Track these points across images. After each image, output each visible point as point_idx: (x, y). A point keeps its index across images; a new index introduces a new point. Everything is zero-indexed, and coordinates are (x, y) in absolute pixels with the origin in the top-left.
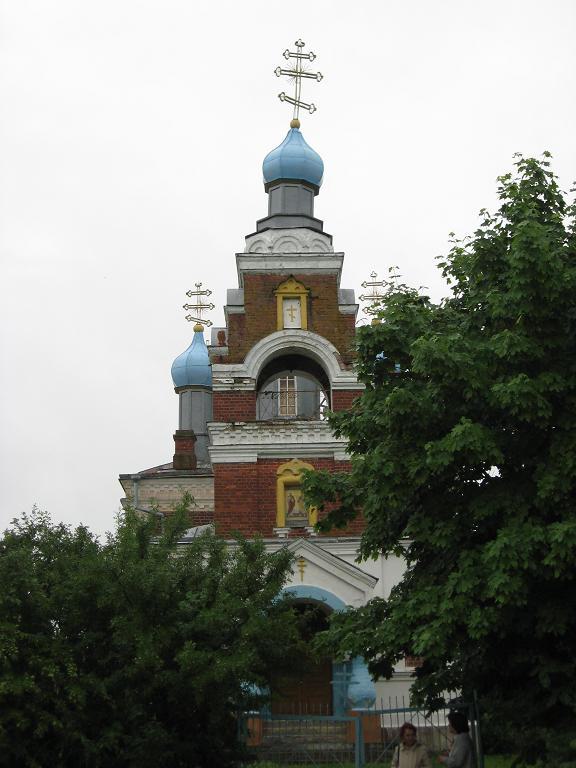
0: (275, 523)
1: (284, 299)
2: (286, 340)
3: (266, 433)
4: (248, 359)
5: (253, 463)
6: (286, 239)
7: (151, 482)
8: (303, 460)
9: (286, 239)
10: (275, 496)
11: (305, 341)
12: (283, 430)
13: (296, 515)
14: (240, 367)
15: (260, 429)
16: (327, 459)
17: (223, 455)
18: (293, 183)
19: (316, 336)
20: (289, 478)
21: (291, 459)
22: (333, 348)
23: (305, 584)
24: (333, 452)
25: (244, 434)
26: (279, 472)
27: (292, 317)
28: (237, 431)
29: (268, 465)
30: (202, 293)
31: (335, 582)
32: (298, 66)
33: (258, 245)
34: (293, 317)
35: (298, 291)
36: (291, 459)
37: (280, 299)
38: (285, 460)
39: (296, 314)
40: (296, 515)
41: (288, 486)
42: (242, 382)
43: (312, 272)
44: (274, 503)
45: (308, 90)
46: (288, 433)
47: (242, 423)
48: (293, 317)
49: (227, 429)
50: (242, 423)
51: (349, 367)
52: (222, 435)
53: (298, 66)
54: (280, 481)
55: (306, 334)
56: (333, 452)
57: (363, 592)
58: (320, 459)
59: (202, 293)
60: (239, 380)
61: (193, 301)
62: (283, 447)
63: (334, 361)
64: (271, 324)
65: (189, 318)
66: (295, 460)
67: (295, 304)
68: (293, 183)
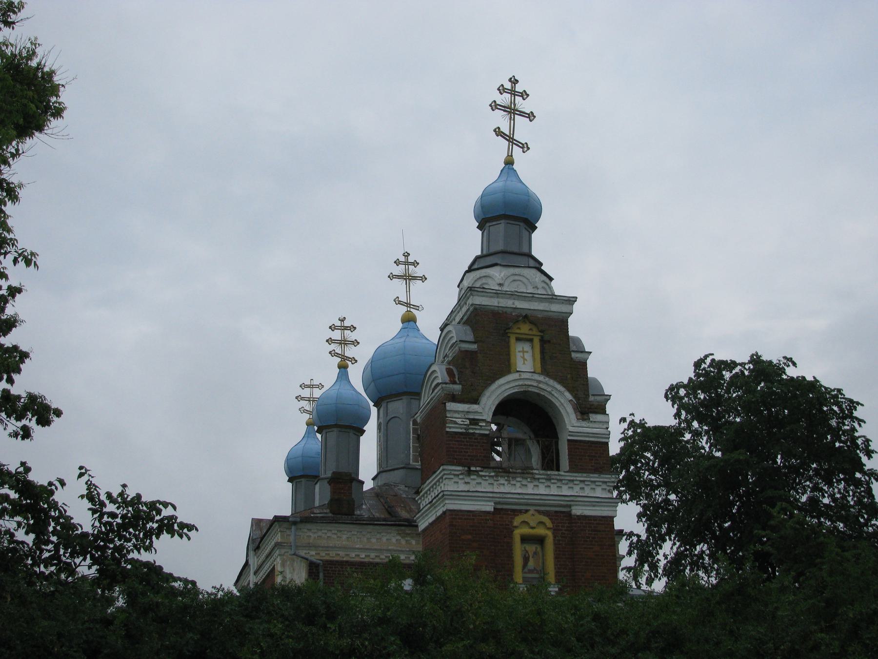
0: (512, 579)
1: (518, 339)
2: (521, 383)
3: (502, 481)
4: (483, 400)
5: (488, 512)
6: (516, 278)
7: (309, 526)
8: (539, 512)
9: (516, 278)
10: (511, 550)
11: (541, 385)
12: (519, 479)
13: (531, 571)
14: (475, 407)
15: (496, 476)
16: (561, 512)
17: (453, 502)
18: (509, 219)
19: (552, 382)
20: (526, 530)
21: (527, 511)
22: (569, 396)
24: (570, 506)
25: (479, 480)
27: (525, 360)
28: (472, 477)
29: (504, 515)
30: (346, 328)
32: (512, 101)
33: (484, 280)
34: (525, 360)
35: (530, 332)
36: (527, 511)
37: (513, 340)
38: (520, 512)
39: (528, 356)
40: (531, 571)
41: (525, 539)
42: (477, 424)
44: (510, 557)
45: (523, 129)
46: (524, 482)
47: (478, 469)
48: (525, 360)
49: (462, 474)
51: (586, 417)
52: (456, 479)
53: (512, 101)
54: (517, 533)
55: (541, 378)
56: (570, 506)
58: (556, 512)
59: (346, 328)
60: (474, 422)
61: (337, 335)
62: (521, 496)
63: (570, 409)
64: (505, 367)
65: (332, 353)
66: (531, 512)
67: (527, 347)
68: (509, 219)
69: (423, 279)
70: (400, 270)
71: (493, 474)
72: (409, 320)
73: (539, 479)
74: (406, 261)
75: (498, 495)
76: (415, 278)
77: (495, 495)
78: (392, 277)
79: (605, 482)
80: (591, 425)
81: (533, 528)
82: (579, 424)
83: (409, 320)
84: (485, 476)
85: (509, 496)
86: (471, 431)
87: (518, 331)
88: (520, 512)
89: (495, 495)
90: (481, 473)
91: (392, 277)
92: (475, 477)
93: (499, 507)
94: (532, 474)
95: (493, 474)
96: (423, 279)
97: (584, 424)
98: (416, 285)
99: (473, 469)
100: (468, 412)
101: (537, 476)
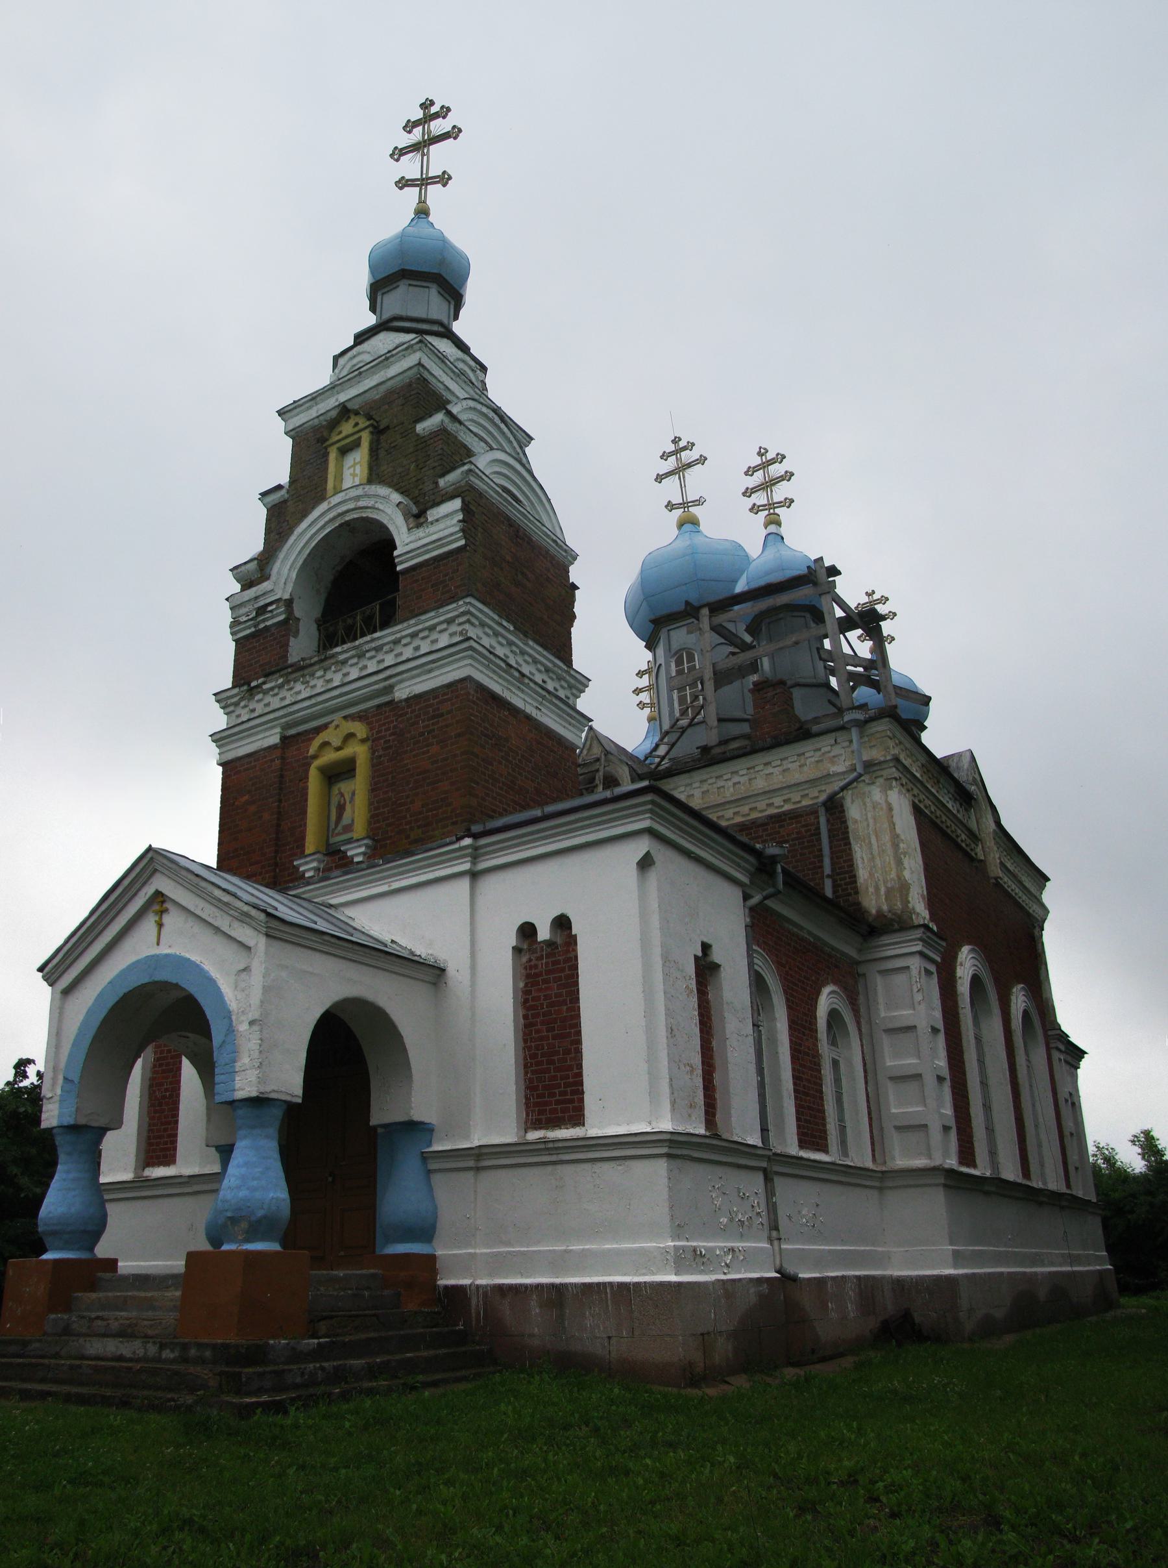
3: (299, 687)
9: (355, 361)
11: (361, 504)
15: (288, 682)
18: (418, 283)
20: (329, 757)
22: (396, 497)
23: (164, 950)
26: (312, 751)
31: (207, 936)
43: (383, 389)
45: (440, 157)
47: (260, 681)
49: (242, 699)
50: (260, 681)
51: (422, 520)
57: (249, 948)
58: (379, 706)
62: (313, 701)
68: (418, 283)
69: (702, 460)
70: (671, 463)
71: (281, 681)
72: (689, 523)
73: (344, 662)
74: (679, 447)
75: (281, 713)
76: (689, 465)
77: (277, 714)
78: (660, 478)
79: (449, 622)
80: (432, 529)
81: (338, 749)
82: (413, 538)
83: (689, 523)
84: (272, 689)
85: (296, 707)
86: (262, 626)
87: (340, 437)
88: (318, 730)
89: (277, 714)
90: (265, 687)
91: (660, 478)
92: (260, 696)
93: (293, 732)
94: (333, 656)
95: (281, 681)
96: (702, 460)
97: (420, 532)
98: (691, 475)
99: (253, 684)
100: (256, 598)
101: (341, 657)
